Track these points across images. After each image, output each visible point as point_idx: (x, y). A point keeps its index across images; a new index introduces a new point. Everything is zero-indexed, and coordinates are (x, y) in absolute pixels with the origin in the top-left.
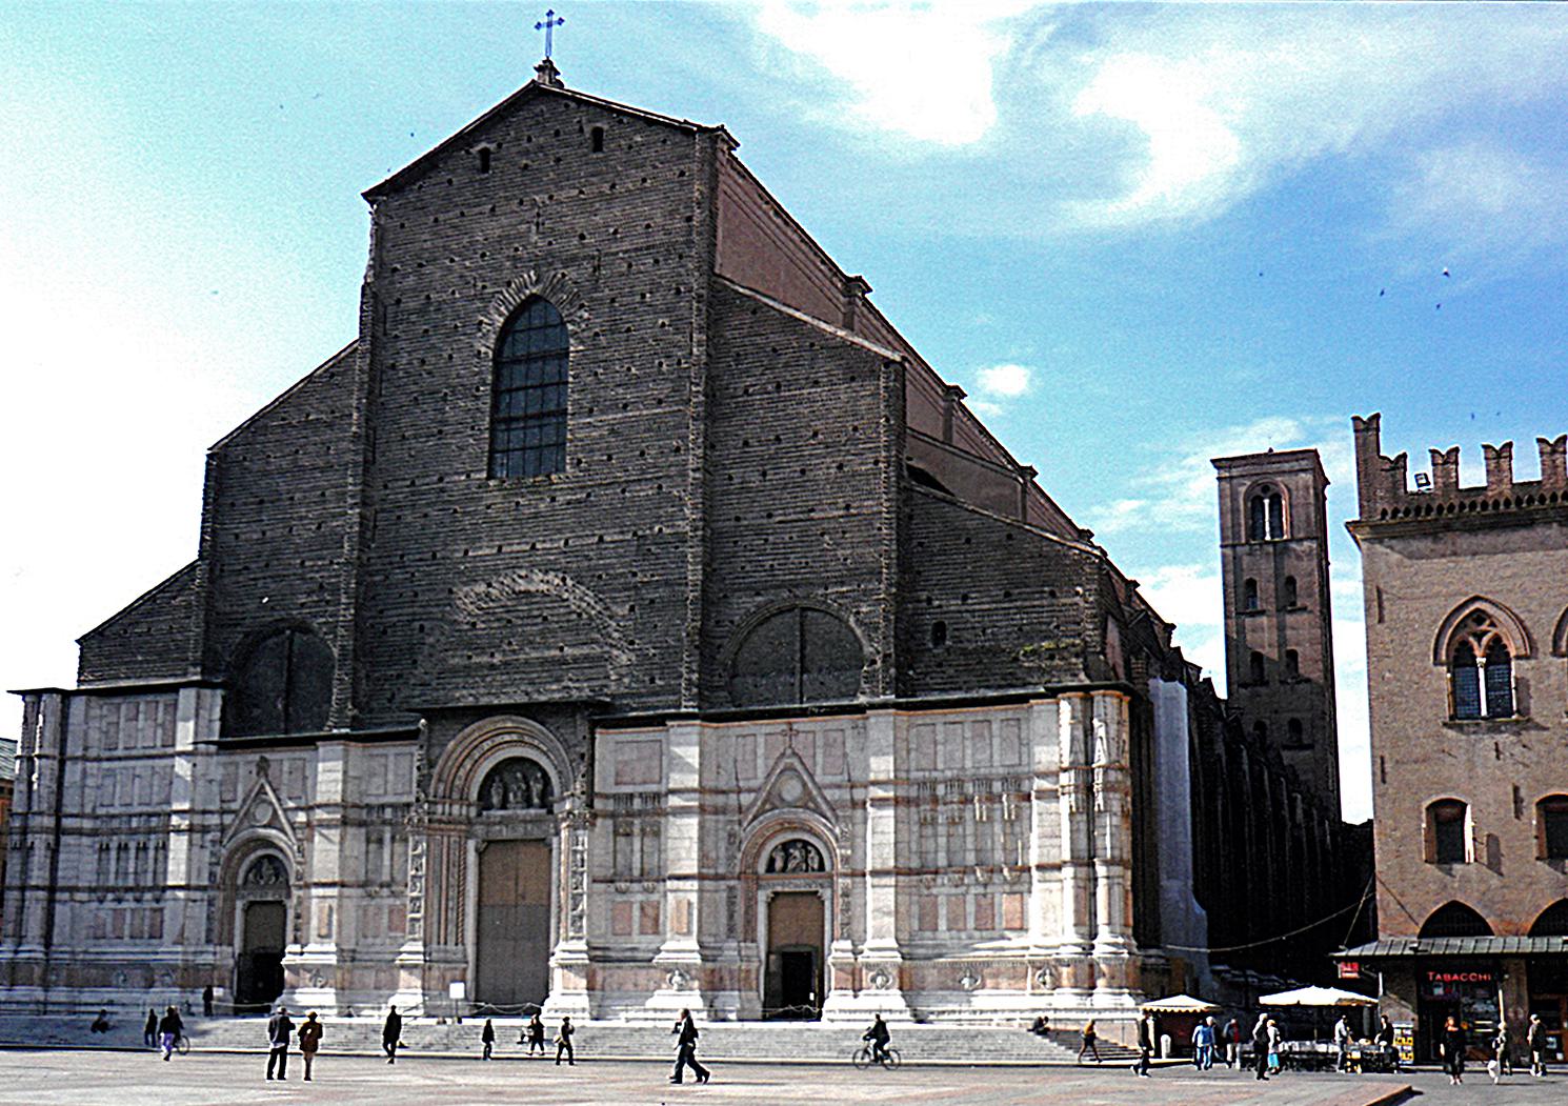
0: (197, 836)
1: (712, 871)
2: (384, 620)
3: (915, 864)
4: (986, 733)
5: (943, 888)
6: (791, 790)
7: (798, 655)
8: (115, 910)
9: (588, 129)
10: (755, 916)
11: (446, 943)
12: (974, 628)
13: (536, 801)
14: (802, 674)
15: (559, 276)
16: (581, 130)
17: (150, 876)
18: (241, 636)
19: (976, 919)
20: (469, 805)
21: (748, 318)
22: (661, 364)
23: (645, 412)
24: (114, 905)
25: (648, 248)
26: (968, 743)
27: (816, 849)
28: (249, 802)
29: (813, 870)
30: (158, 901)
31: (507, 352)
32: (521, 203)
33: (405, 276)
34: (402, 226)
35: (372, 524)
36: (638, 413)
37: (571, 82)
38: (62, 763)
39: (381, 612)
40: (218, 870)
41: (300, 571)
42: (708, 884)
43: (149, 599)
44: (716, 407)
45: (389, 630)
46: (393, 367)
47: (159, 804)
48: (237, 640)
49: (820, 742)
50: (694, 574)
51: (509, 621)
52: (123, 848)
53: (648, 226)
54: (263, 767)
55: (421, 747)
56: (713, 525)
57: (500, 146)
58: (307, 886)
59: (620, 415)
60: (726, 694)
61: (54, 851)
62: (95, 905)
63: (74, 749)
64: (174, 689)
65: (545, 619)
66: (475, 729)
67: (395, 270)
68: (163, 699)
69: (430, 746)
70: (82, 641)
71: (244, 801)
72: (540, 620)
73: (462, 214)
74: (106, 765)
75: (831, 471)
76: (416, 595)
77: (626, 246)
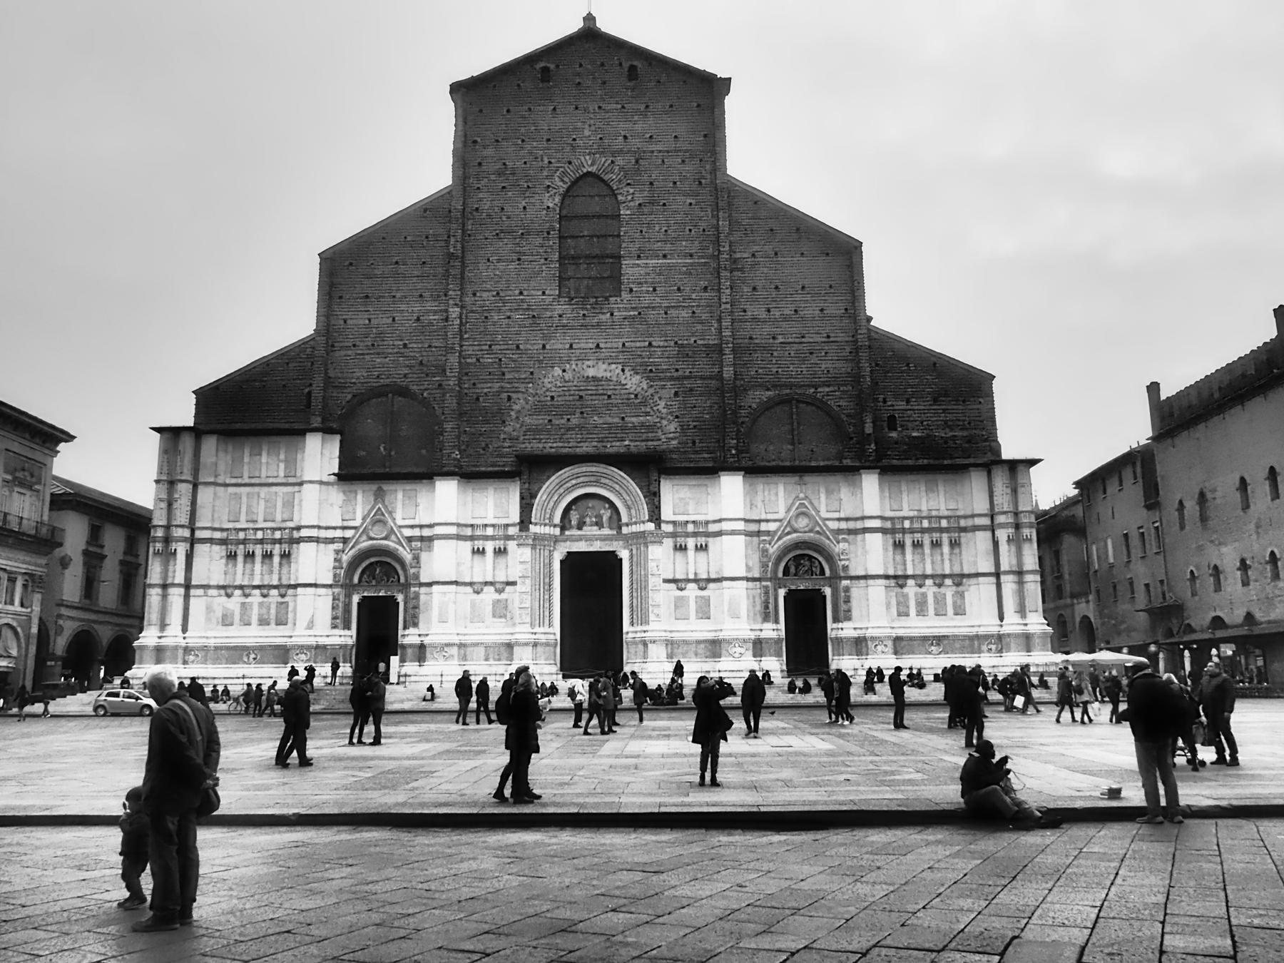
0: (322, 545)
1: (750, 575)
3: (891, 572)
5: (911, 588)
6: (802, 523)
9: (626, 65)
16: (621, 64)
18: (349, 397)
19: (935, 609)
20: (555, 526)
22: (690, 230)
24: (243, 600)
25: (676, 151)
26: (924, 494)
28: (368, 520)
30: (283, 596)
32: (577, 108)
33: (485, 147)
38: (195, 486)
39: (474, 384)
41: (402, 351)
42: (751, 584)
45: (481, 399)
46: (477, 209)
47: (284, 521)
49: (822, 490)
50: (728, 372)
51: (581, 397)
52: (250, 556)
53: (676, 137)
54: (379, 495)
57: (557, 66)
58: (421, 585)
61: (189, 558)
62: (224, 599)
63: (201, 480)
66: (565, 472)
67: (475, 142)
68: (284, 440)
71: (364, 519)
73: (530, 109)
74: (231, 490)
76: (504, 374)
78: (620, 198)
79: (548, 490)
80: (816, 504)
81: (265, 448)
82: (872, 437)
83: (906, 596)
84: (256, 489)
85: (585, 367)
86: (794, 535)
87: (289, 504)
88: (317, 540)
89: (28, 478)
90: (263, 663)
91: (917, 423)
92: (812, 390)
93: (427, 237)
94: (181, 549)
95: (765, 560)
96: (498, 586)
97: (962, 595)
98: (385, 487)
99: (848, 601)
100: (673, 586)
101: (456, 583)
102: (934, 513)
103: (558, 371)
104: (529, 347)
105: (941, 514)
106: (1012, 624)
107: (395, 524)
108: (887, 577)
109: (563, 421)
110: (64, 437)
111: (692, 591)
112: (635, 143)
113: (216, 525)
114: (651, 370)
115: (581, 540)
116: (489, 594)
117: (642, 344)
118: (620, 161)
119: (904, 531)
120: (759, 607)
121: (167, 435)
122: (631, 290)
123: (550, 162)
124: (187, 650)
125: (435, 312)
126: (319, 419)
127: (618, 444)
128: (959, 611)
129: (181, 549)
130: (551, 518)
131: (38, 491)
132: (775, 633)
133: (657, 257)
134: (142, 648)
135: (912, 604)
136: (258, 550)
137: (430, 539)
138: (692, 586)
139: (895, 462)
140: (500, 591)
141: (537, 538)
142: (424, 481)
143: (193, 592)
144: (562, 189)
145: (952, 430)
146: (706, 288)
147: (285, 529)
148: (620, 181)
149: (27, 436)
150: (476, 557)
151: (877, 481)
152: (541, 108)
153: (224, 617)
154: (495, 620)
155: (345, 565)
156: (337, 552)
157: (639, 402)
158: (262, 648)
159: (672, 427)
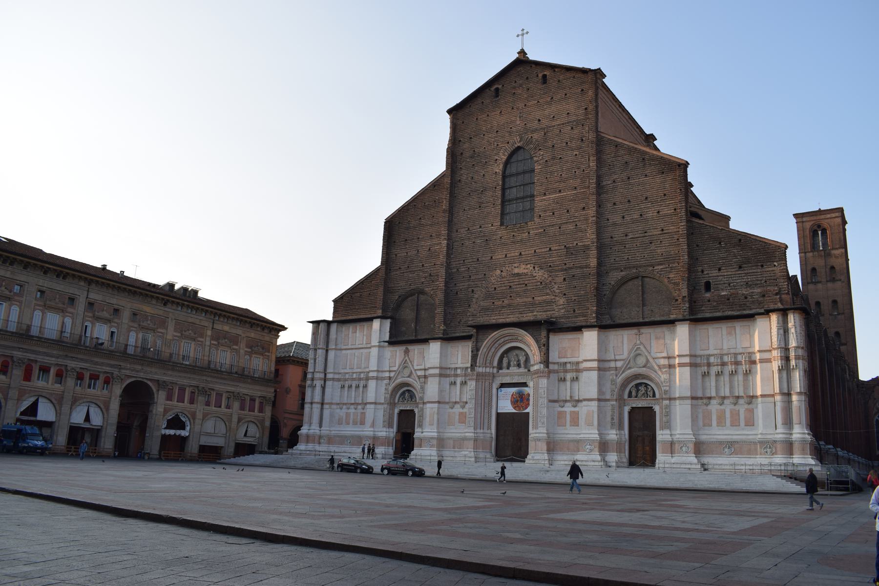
0: (379, 381)
1: (603, 397)
2: (457, 288)
3: (700, 394)
4: (733, 332)
5: (714, 406)
6: (641, 361)
7: (641, 298)
8: (346, 413)
9: (540, 75)
10: (623, 418)
11: (483, 429)
12: (724, 283)
13: (522, 366)
14: (644, 305)
15: (530, 137)
16: (537, 76)
17: (361, 398)
18: (397, 297)
19: (731, 421)
20: (493, 368)
21: (613, 148)
22: (575, 172)
23: (568, 193)
25: (568, 123)
27: (651, 387)
29: (650, 397)
31: (507, 172)
32: (513, 108)
34: (463, 123)
35: (451, 247)
36: (565, 194)
37: (532, 56)
39: (455, 284)
40: (388, 396)
42: (602, 403)
43: (361, 283)
44: (600, 189)
45: (458, 293)
46: (460, 180)
48: (396, 299)
50: (593, 262)
51: (510, 287)
52: (350, 387)
53: (568, 113)
54: (407, 352)
55: (474, 342)
56: (600, 241)
57: (503, 85)
58: (424, 403)
59: (557, 195)
60: (608, 316)
61: (323, 388)
62: (338, 410)
64: (371, 320)
65: (526, 285)
66: (496, 334)
67: (460, 141)
68: (366, 324)
69: (477, 342)
70: (336, 301)
72: (524, 285)
73: (488, 115)
74: (344, 352)
75: (655, 214)
76: (470, 277)
77: (558, 122)
78: (535, 159)
79: (488, 345)
80: (648, 348)
81: (358, 328)
82: (687, 299)
83: (710, 413)
84: (354, 351)
85: (513, 268)
86: (633, 370)
87: (368, 358)
88: (377, 378)
89: (261, 350)
90: (353, 445)
91: (726, 285)
92: (651, 268)
93: (435, 201)
94: (318, 384)
95: (614, 387)
96: (462, 404)
97: (751, 412)
98: (411, 347)
99: (668, 414)
100: (557, 405)
101: (439, 402)
102: (732, 351)
103: (498, 272)
104: (484, 259)
105: (737, 352)
106: (780, 434)
107: (413, 368)
108: (693, 398)
109: (500, 303)
110: (280, 328)
111: (568, 408)
112: (545, 122)
113: (336, 371)
114: (550, 266)
115: (507, 376)
116: (458, 409)
117: (546, 250)
118: (535, 136)
119: (709, 365)
120: (609, 419)
121: (315, 325)
122: (540, 216)
123: (498, 145)
124: (320, 437)
125: (438, 244)
126: (381, 311)
127: (530, 314)
128: (750, 422)
129: (318, 384)
130: (491, 362)
131: (268, 356)
132: (618, 435)
133: (555, 192)
134: (301, 434)
135: (714, 418)
136: (354, 385)
137: (425, 377)
138: (568, 404)
139: (708, 315)
140: (463, 407)
141: (478, 375)
142: (427, 343)
143: (326, 406)
144: (504, 160)
145: (751, 289)
146: (584, 208)
147: (365, 372)
148: (535, 148)
149: (259, 329)
150: (453, 387)
151: (688, 329)
152: (493, 113)
153: (339, 419)
154: (460, 424)
155: (390, 392)
156: (386, 385)
157: (544, 286)
158: (352, 437)
159: (562, 301)
